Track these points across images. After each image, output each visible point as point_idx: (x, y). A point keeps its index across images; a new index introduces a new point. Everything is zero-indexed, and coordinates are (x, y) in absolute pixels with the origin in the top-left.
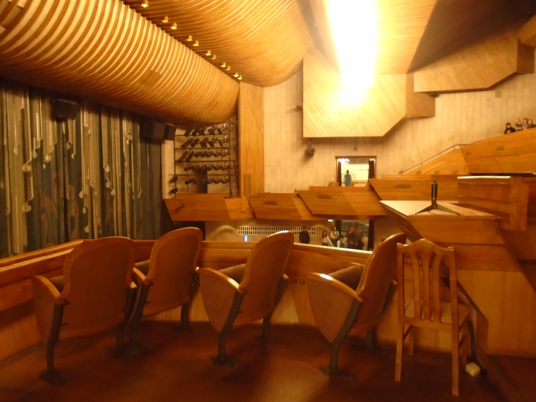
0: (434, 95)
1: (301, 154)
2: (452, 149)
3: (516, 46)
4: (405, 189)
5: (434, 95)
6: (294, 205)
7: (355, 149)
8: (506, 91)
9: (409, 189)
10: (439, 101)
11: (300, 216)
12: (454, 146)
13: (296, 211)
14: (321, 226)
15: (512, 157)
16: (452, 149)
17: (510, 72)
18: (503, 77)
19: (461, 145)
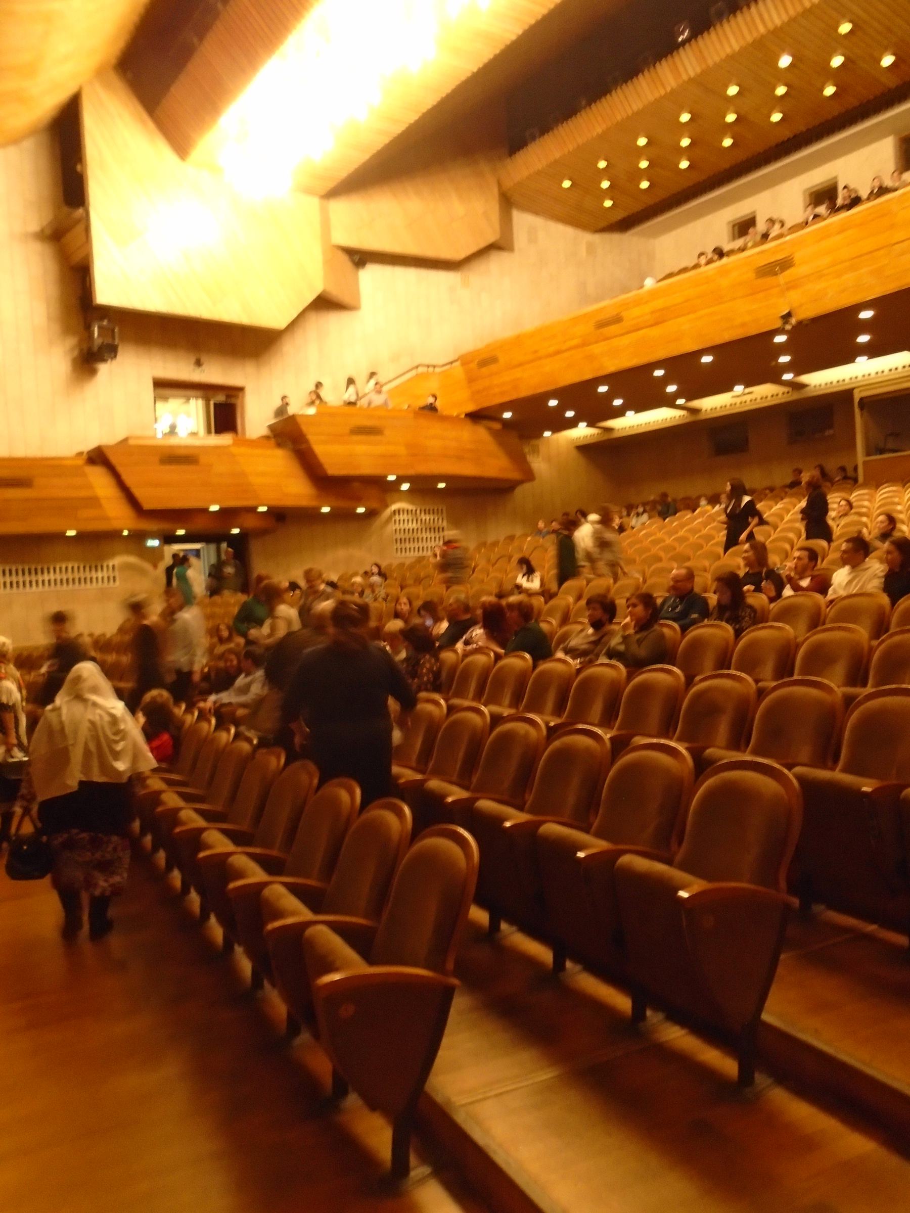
0: (360, 258)
1: (58, 359)
2: (414, 373)
3: (496, 191)
4: (372, 438)
5: (360, 258)
6: (90, 487)
7: (198, 363)
8: (477, 275)
9: (378, 438)
10: (371, 277)
11: (106, 518)
12: (417, 367)
13: (93, 502)
14: (132, 559)
15: (641, 332)
16: (414, 373)
17: (491, 236)
18: (482, 244)
19: (428, 366)
